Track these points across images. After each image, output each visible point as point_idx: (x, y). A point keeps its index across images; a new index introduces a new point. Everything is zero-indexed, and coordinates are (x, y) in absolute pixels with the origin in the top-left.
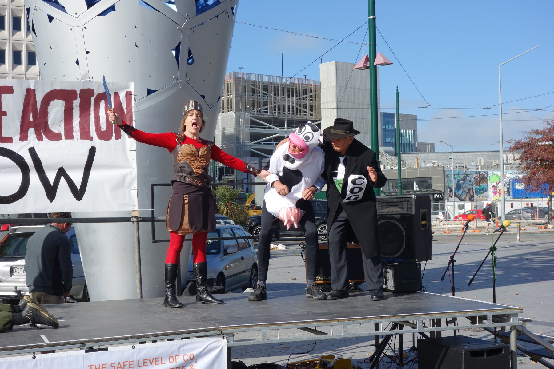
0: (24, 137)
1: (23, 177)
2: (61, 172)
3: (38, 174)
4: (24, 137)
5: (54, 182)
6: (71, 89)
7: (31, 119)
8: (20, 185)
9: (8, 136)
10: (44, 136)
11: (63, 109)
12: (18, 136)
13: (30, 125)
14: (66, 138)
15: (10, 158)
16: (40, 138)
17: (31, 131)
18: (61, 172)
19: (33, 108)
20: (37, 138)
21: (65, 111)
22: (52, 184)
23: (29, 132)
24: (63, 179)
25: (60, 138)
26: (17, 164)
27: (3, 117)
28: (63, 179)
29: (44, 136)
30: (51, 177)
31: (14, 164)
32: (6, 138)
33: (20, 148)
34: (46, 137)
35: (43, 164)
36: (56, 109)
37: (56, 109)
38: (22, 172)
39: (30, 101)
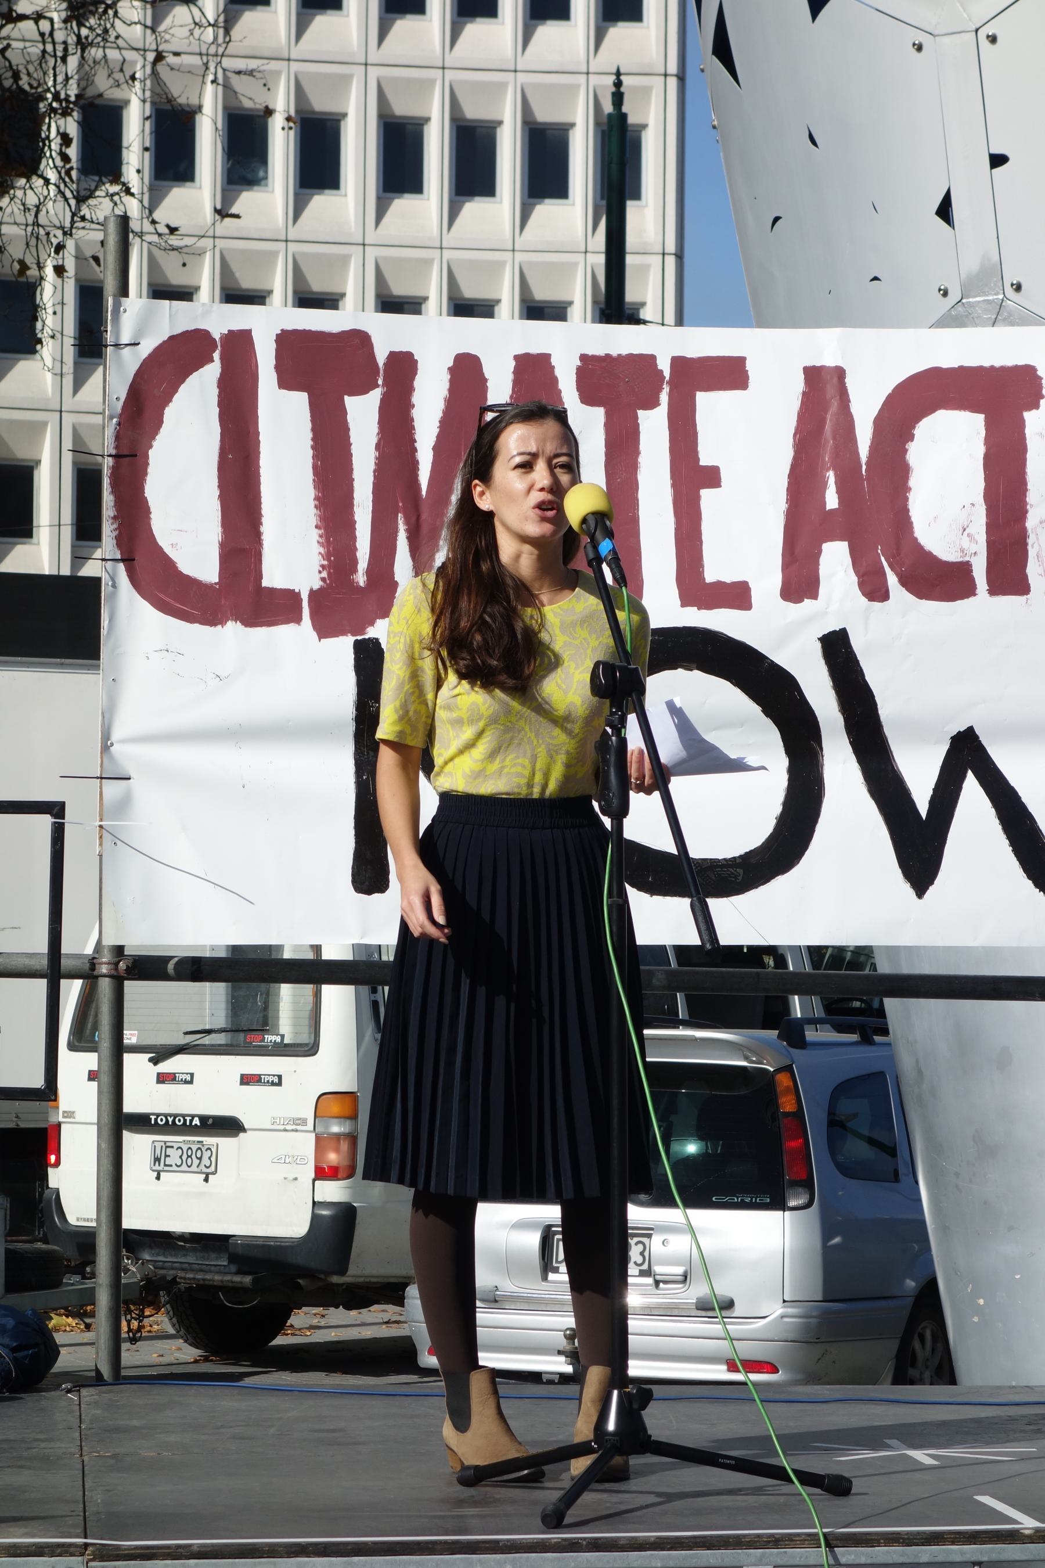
0: (800, 582)
1: (791, 770)
2: (966, 754)
3: (861, 760)
4: (800, 582)
5: (933, 802)
6: (1010, 362)
7: (832, 500)
8: (778, 809)
9: (728, 579)
10: (892, 579)
11: (980, 450)
12: (776, 579)
13: (830, 527)
14: (995, 589)
15: (737, 684)
16: (874, 590)
17: (835, 559)
18: (966, 754)
19: (836, 455)
20: (862, 585)
21: (990, 462)
22: (923, 808)
23: (823, 560)
24: (971, 788)
25: (968, 590)
26: (767, 712)
27: (705, 493)
28: (971, 788)
29: (892, 579)
30: (920, 773)
31: (756, 709)
32: (719, 585)
33: (784, 634)
34: (906, 582)
35: (886, 711)
36: (948, 453)
37: (948, 453)
38: (788, 752)
39: (822, 422)
